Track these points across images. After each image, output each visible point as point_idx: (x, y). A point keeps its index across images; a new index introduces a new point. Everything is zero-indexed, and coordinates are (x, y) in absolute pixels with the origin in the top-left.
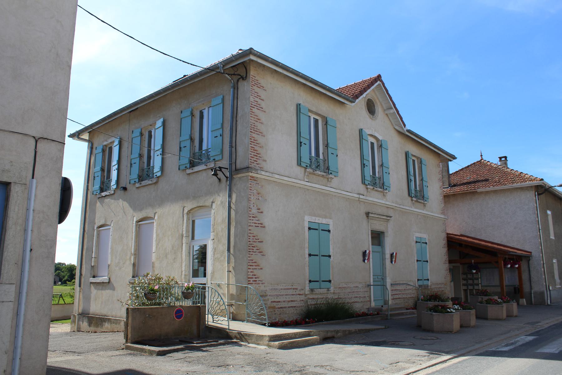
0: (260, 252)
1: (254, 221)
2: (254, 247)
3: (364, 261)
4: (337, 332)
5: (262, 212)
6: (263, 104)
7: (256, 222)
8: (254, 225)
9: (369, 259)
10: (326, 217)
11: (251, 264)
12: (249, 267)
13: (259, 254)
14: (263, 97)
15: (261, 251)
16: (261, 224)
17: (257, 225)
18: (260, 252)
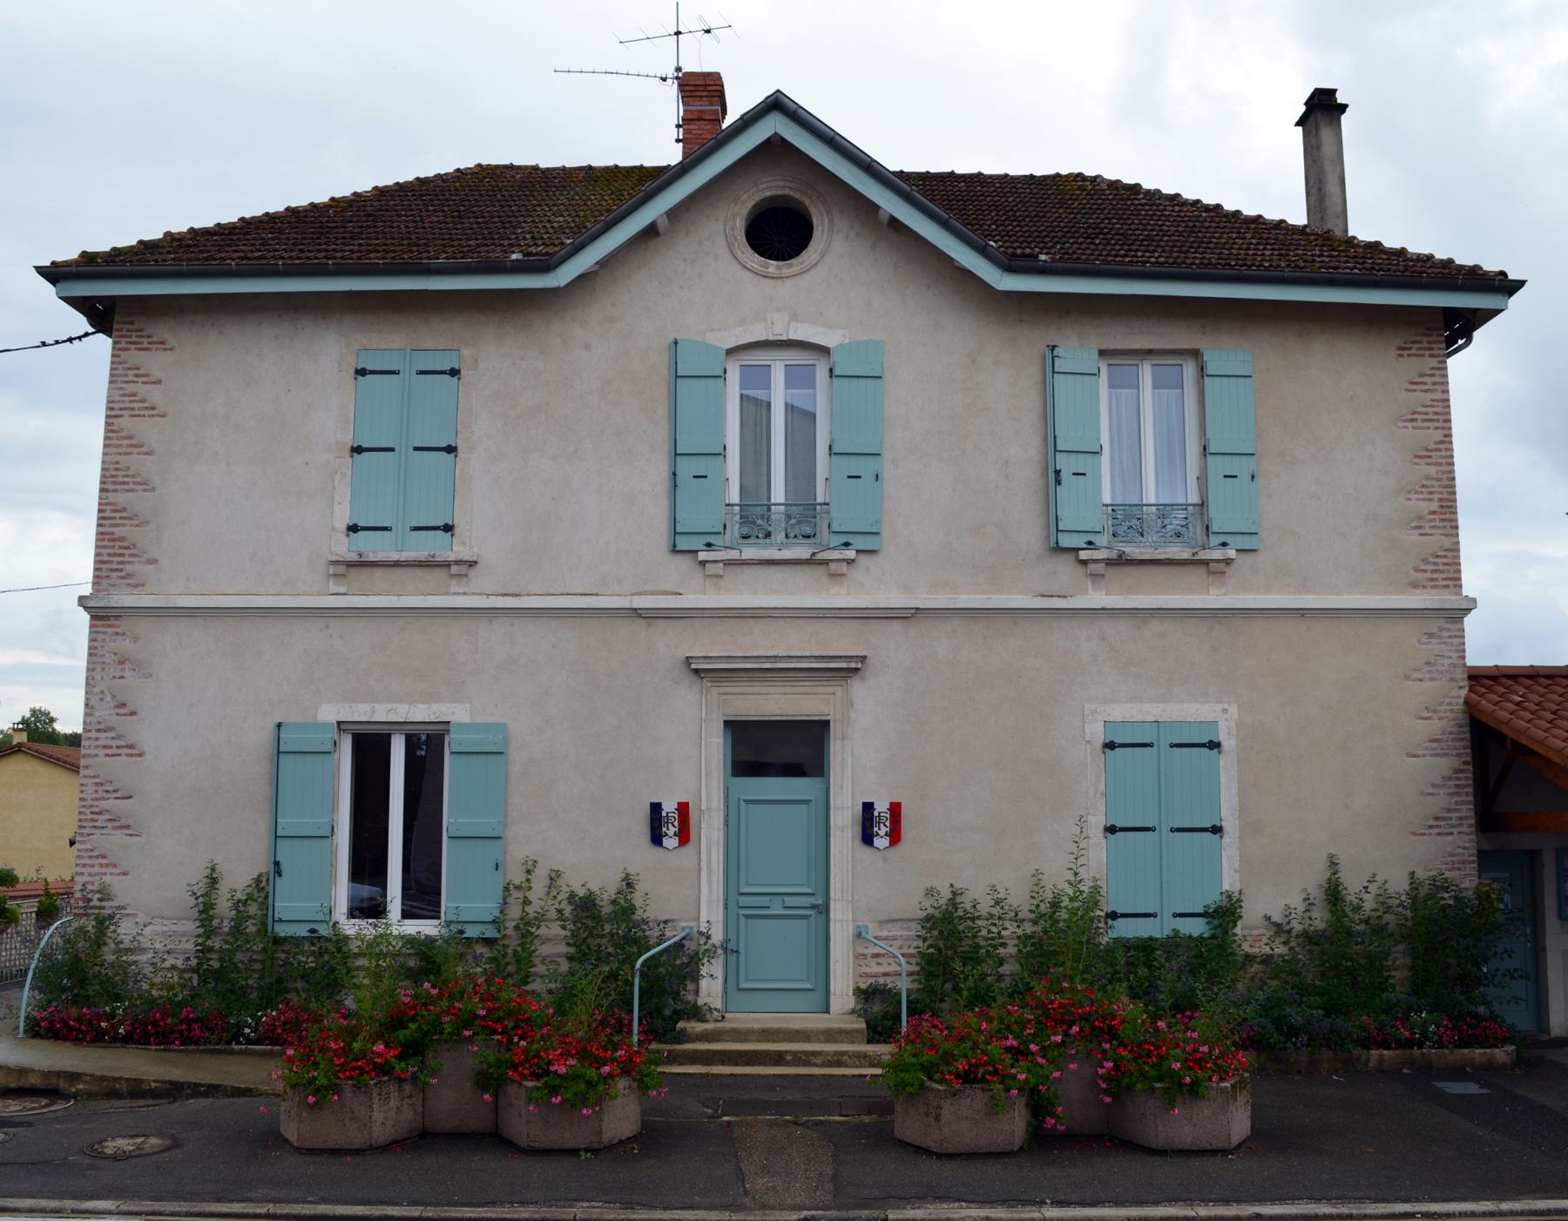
0: (123, 827)
1: (100, 743)
2: (100, 813)
3: (657, 839)
4: (73, 1077)
5: (133, 713)
6: (155, 395)
7: (114, 743)
8: (102, 752)
9: (684, 836)
10: (430, 697)
11: (87, 861)
12: (80, 870)
13: (118, 832)
14: (157, 374)
15: (124, 822)
16: (131, 747)
17: (114, 751)
18: (123, 827)
